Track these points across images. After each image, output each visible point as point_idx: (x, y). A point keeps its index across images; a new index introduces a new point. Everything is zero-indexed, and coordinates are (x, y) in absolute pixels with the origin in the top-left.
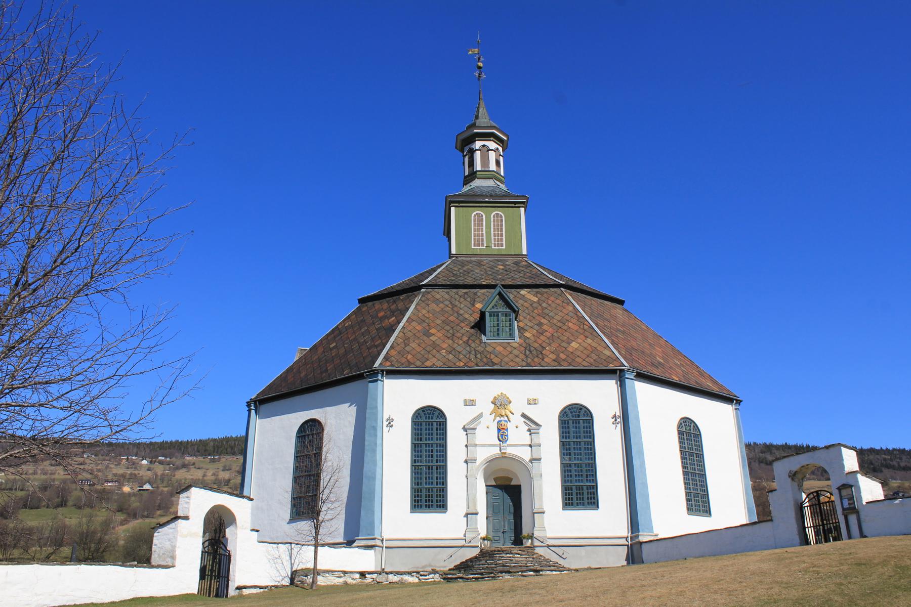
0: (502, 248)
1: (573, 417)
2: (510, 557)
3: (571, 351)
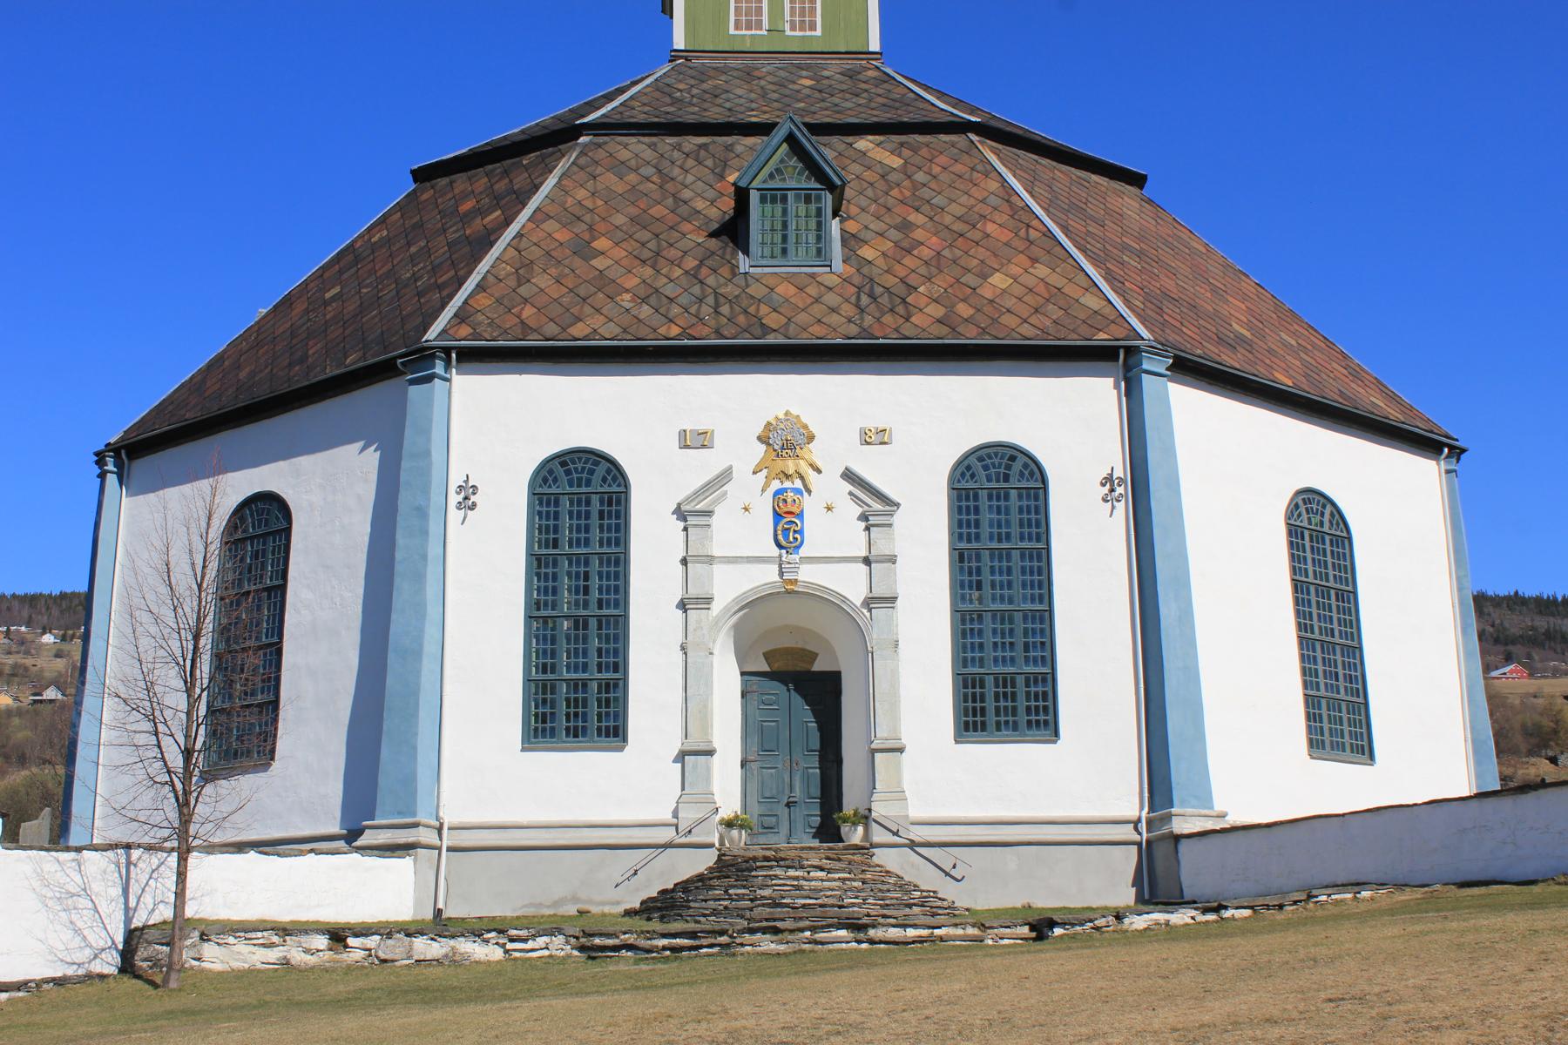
0: (813, 33)
1: (989, 480)
2: (796, 878)
3: (989, 295)
